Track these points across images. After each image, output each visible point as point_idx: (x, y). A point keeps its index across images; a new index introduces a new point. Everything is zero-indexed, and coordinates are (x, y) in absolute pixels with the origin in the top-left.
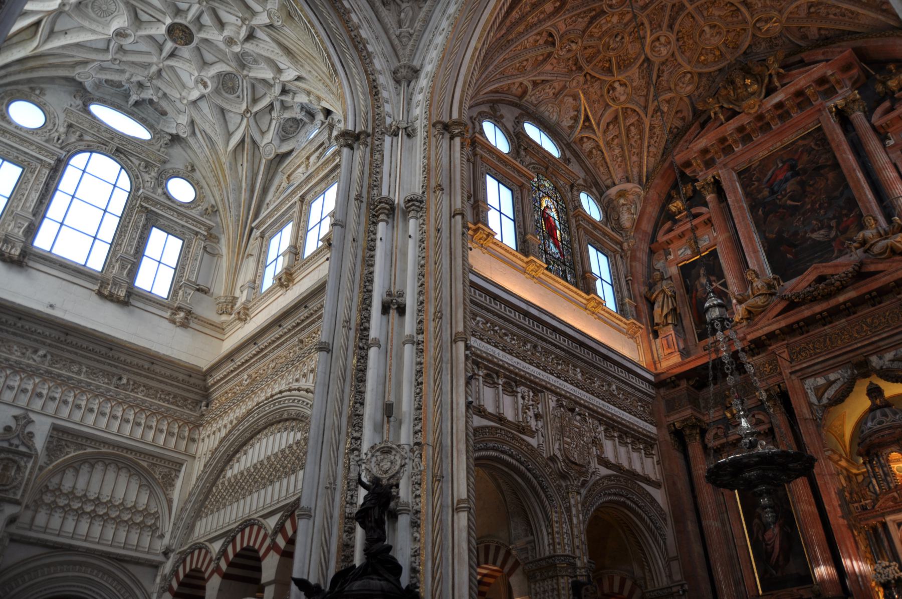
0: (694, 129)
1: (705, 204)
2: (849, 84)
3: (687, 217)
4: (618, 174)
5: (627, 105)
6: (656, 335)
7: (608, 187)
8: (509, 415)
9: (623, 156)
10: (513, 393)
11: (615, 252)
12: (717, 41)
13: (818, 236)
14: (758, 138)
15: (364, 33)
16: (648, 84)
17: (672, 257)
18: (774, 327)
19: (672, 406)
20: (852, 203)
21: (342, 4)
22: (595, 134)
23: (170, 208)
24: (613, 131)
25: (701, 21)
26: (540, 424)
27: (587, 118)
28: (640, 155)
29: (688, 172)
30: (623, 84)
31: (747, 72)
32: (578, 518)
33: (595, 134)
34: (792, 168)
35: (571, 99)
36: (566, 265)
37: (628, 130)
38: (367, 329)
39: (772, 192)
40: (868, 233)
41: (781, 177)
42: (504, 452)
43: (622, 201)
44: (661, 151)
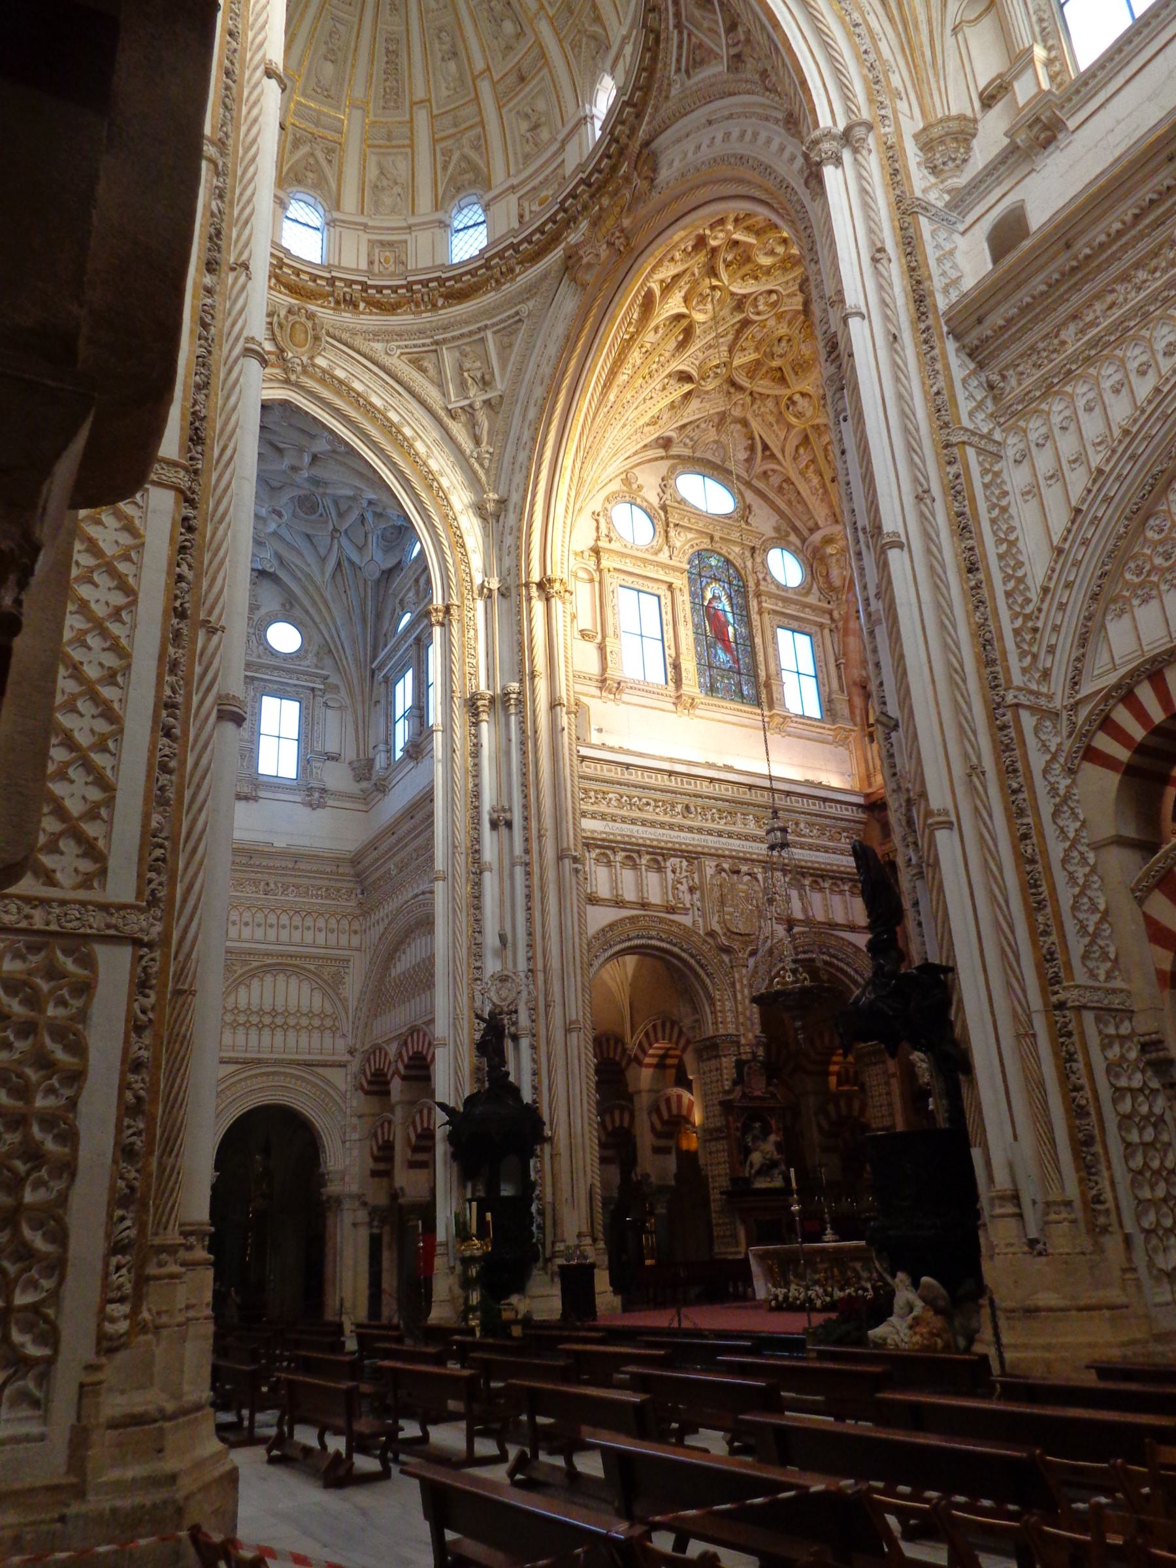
7: (812, 531)
8: (655, 897)
10: (660, 869)
11: (821, 626)
15: (433, 465)
21: (403, 435)
22: (780, 464)
23: (276, 668)
24: (805, 457)
26: (697, 895)
32: (742, 992)
33: (780, 464)
35: (739, 426)
36: (739, 673)
38: (477, 851)
42: (651, 938)
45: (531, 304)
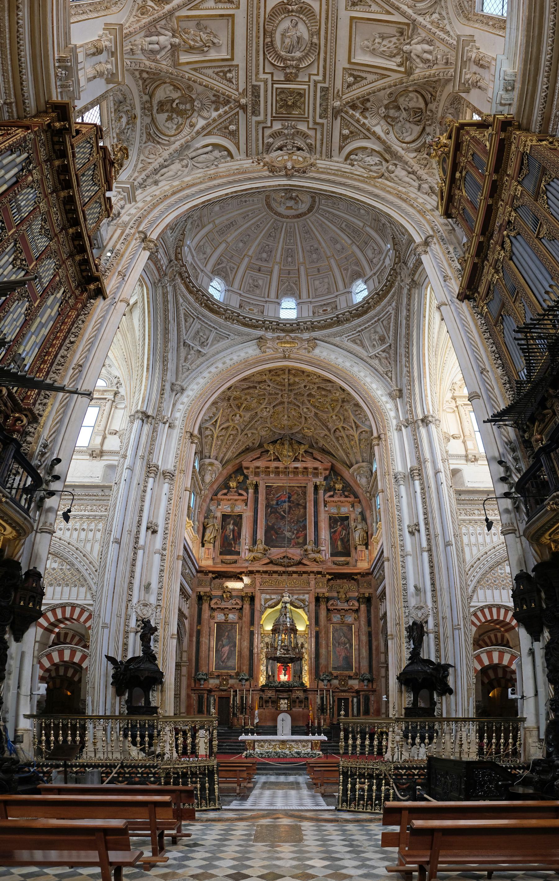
0: (257, 454)
1: (247, 490)
2: (324, 476)
3: (235, 492)
4: (213, 454)
5: (237, 426)
6: (203, 545)
9: (221, 446)
12: (286, 422)
13: (288, 534)
14: (282, 476)
16: (250, 422)
17: (220, 507)
18: (261, 569)
19: (200, 584)
20: (305, 528)
25: (286, 412)
27: (216, 421)
28: (228, 449)
29: (245, 471)
30: (240, 416)
31: (291, 444)
34: (289, 498)
37: (229, 436)
39: (277, 504)
40: (309, 547)
41: (283, 499)
43: (210, 468)
44: (237, 453)
45: (236, 337)
